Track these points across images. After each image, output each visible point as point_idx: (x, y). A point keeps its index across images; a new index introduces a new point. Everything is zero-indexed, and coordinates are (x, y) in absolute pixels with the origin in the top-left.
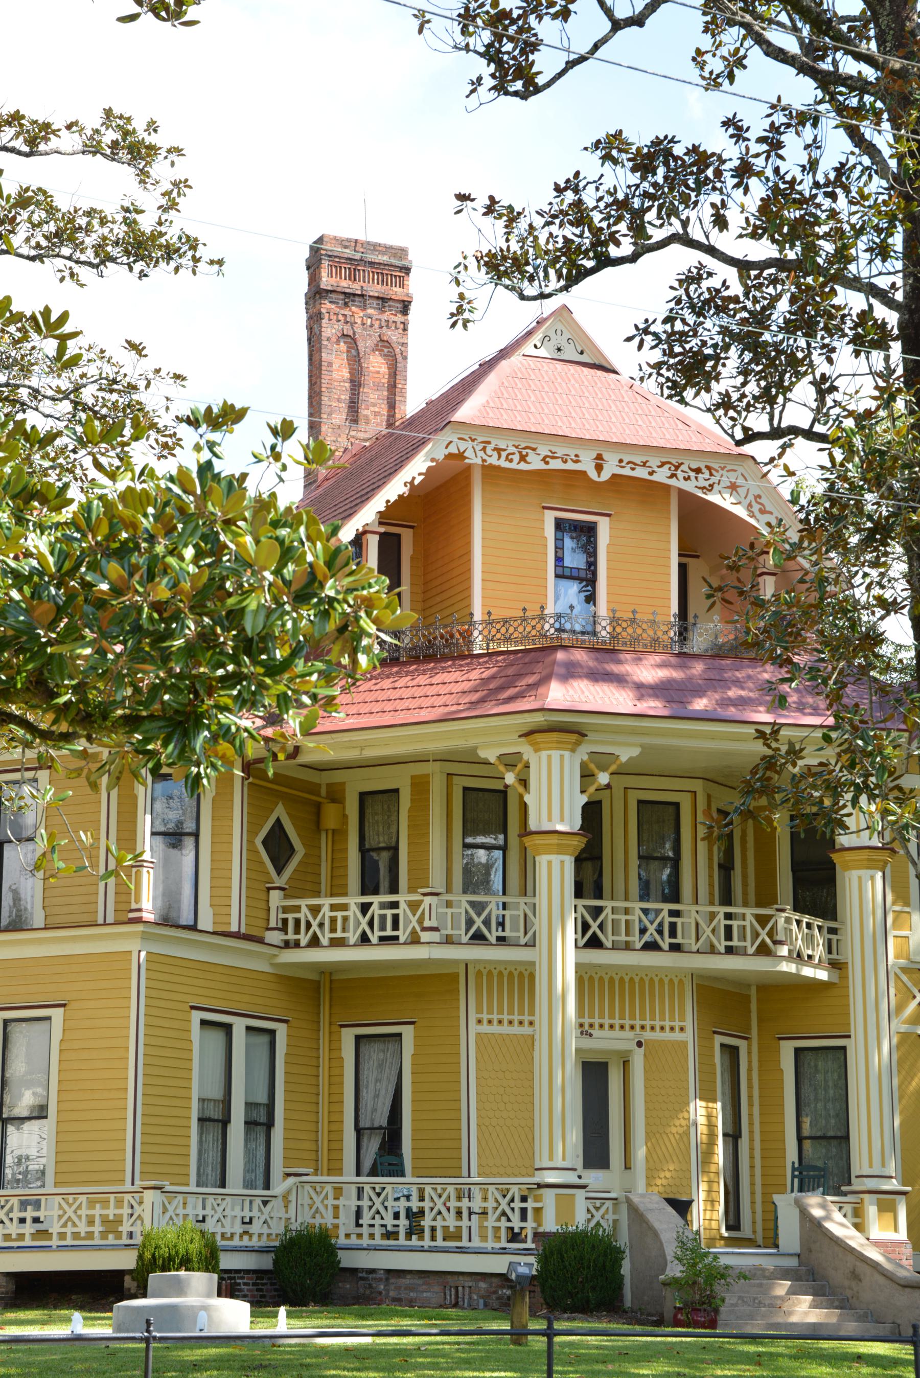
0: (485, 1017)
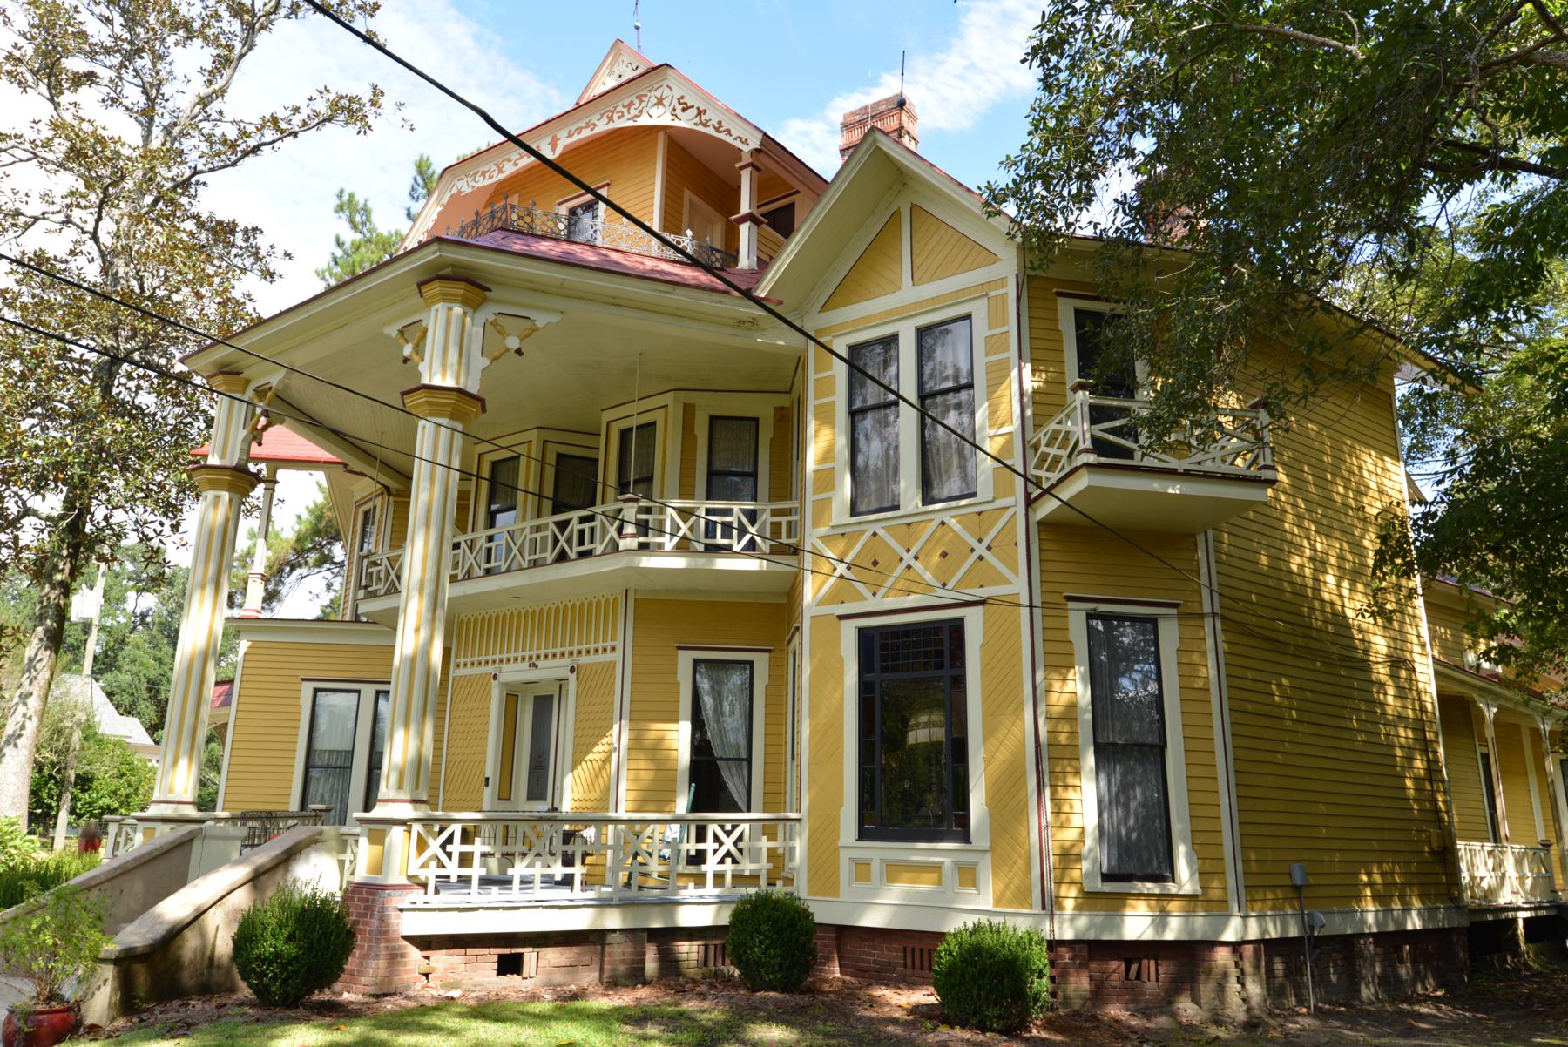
0: (462, 661)
